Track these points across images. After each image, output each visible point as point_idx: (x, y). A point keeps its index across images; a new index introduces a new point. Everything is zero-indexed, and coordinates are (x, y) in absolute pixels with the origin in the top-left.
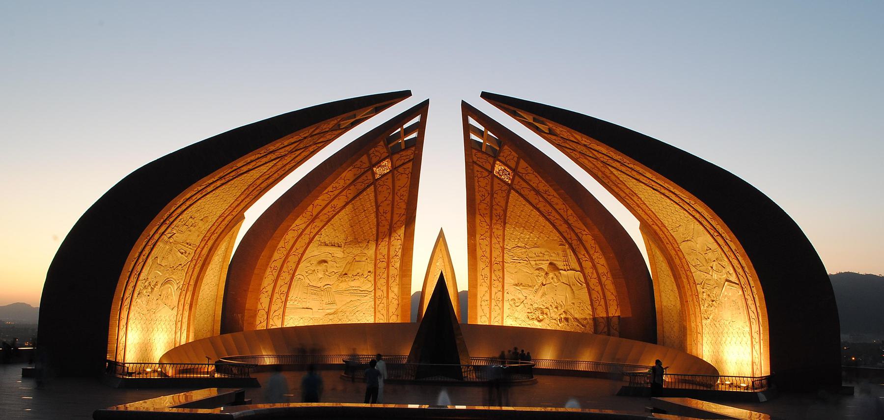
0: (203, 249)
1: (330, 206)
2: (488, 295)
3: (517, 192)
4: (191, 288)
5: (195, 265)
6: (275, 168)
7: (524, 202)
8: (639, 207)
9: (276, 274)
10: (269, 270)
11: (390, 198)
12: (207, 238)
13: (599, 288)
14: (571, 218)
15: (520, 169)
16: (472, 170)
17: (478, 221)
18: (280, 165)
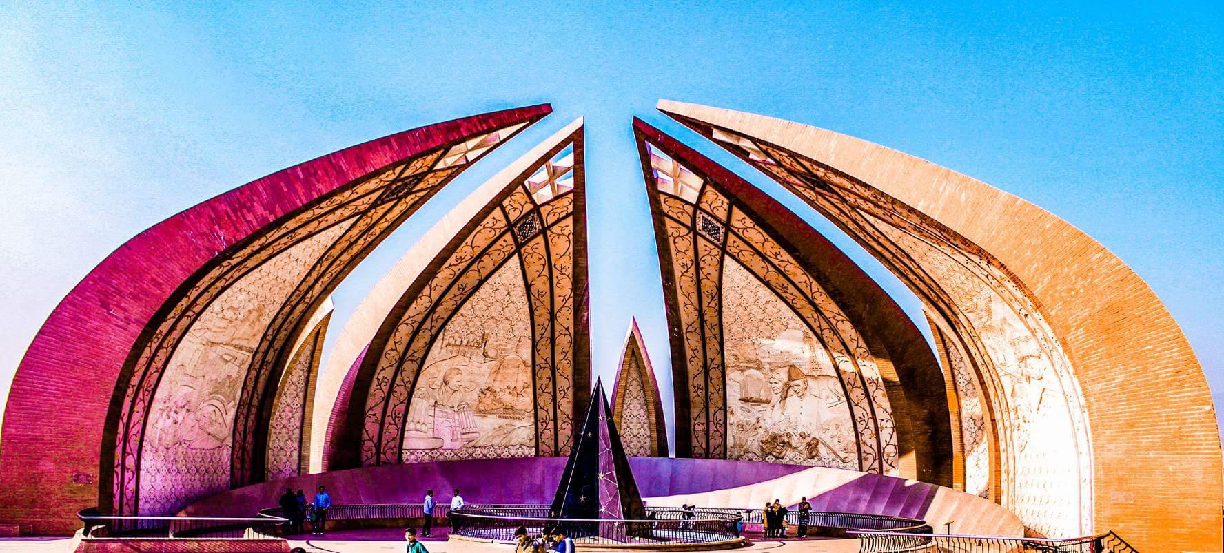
0: (266, 353)
1: (455, 286)
2: (703, 415)
3: (733, 257)
4: (254, 410)
5: (257, 378)
6: (355, 232)
7: (747, 273)
8: (915, 274)
9: (386, 389)
10: (375, 382)
11: (546, 272)
12: (269, 338)
13: (865, 403)
14: (817, 295)
15: (735, 223)
16: (664, 224)
17: (681, 306)
18: (362, 225)
